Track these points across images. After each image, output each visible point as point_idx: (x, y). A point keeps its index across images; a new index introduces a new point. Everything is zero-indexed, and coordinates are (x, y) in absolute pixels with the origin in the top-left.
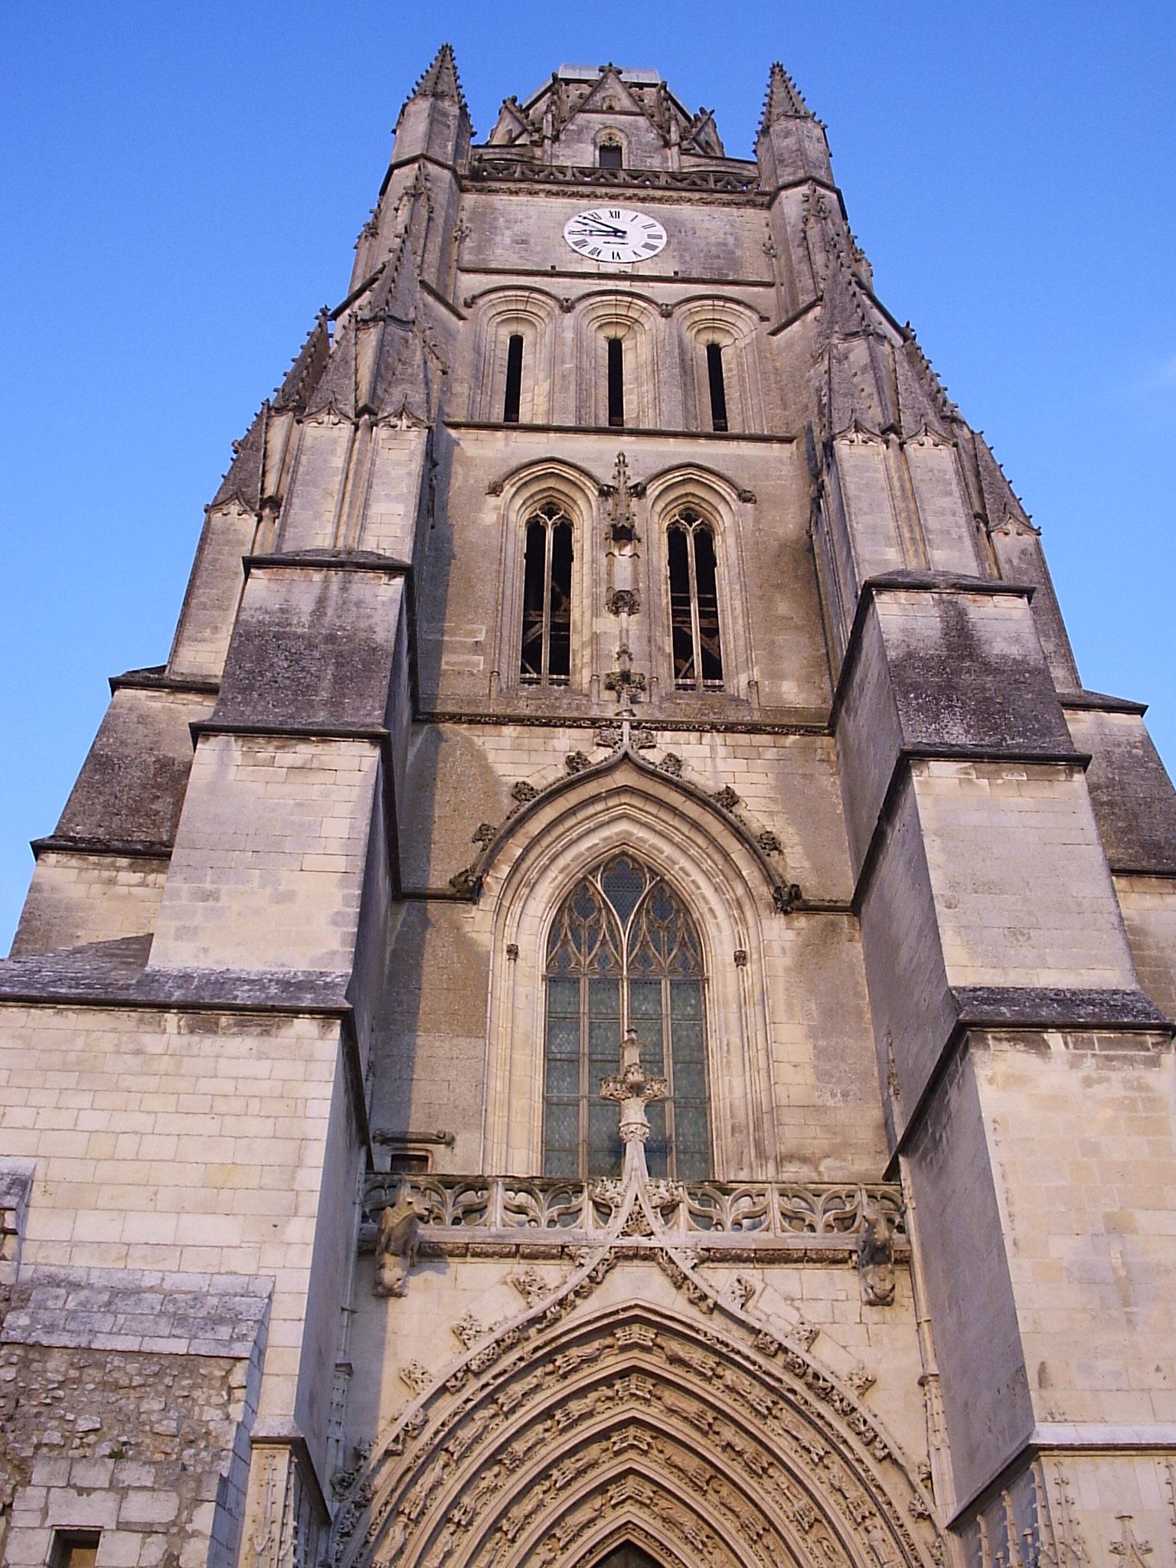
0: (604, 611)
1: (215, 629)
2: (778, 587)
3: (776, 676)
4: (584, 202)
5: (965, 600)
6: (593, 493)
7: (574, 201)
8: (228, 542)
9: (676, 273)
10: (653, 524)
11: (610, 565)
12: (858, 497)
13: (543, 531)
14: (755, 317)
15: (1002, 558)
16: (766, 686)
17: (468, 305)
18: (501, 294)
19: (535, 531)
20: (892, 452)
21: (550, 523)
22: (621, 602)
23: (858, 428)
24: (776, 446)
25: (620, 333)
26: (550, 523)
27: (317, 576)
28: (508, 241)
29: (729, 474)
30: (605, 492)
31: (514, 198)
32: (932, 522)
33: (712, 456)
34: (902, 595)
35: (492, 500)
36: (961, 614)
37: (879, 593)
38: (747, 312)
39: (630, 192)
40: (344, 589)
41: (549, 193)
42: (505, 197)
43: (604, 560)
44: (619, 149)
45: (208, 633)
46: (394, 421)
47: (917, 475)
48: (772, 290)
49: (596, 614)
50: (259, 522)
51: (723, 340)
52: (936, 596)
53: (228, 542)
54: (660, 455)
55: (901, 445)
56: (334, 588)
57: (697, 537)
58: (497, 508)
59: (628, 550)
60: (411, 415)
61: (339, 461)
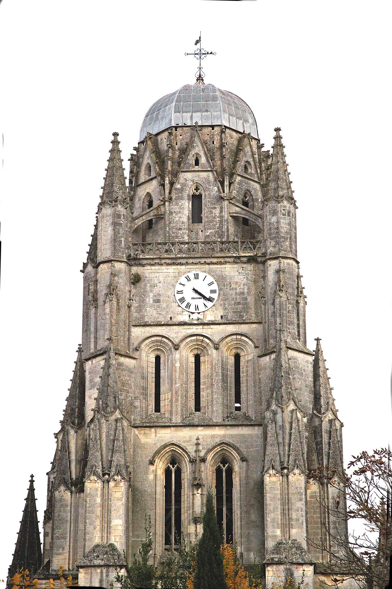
0: (192, 522)
1: (63, 549)
2: (252, 506)
3: (248, 550)
4: (183, 267)
5: (293, 568)
6: (187, 460)
7: (179, 267)
8: (62, 506)
9: (222, 317)
10: (208, 473)
11: (193, 499)
12: (270, 505)
13: (171, 471)
14: (253, 345)
15: (330, 497)
16: (245, 554)
17: (137, 349)
18: (150, 340)
19: (168, 472)
20: (285, 479)
21: (173, 470)
22: (196, 521)
23: (273, 468)
24: (256, 428)
25: (199, 352)
26: (173, 470)
27: (99, 571)
28: (151, 302)
29: (238, 445)
30: (192, 461)
31: (153, 268)
32: (294, 516)
33: (232, 436)
34: (275, 567)
35: (152, 468)
36: (292, 575)
37: (268, 566)
38: (250, 342)
39: (203, 261)
40: (107, 576)
41: (168, 264)
42: (149, 267)
43: (191, 497)
44: (201, 195)
45: (61, 551)
46: (116, 477)
47: (292, 490)
48: (262, 325)
49: (189, 524)
50: (71, 494)
51: (242, 354)
52: (285, 566)
53: (62, 506)
54: (213, 436)
55: (287, 476)
56: (104, 575)
57: (227, 471)
58: (153, 471)
59: (199, 491)
60: (121, 475)
61: (99, 500)
